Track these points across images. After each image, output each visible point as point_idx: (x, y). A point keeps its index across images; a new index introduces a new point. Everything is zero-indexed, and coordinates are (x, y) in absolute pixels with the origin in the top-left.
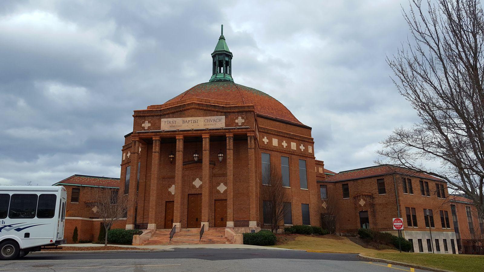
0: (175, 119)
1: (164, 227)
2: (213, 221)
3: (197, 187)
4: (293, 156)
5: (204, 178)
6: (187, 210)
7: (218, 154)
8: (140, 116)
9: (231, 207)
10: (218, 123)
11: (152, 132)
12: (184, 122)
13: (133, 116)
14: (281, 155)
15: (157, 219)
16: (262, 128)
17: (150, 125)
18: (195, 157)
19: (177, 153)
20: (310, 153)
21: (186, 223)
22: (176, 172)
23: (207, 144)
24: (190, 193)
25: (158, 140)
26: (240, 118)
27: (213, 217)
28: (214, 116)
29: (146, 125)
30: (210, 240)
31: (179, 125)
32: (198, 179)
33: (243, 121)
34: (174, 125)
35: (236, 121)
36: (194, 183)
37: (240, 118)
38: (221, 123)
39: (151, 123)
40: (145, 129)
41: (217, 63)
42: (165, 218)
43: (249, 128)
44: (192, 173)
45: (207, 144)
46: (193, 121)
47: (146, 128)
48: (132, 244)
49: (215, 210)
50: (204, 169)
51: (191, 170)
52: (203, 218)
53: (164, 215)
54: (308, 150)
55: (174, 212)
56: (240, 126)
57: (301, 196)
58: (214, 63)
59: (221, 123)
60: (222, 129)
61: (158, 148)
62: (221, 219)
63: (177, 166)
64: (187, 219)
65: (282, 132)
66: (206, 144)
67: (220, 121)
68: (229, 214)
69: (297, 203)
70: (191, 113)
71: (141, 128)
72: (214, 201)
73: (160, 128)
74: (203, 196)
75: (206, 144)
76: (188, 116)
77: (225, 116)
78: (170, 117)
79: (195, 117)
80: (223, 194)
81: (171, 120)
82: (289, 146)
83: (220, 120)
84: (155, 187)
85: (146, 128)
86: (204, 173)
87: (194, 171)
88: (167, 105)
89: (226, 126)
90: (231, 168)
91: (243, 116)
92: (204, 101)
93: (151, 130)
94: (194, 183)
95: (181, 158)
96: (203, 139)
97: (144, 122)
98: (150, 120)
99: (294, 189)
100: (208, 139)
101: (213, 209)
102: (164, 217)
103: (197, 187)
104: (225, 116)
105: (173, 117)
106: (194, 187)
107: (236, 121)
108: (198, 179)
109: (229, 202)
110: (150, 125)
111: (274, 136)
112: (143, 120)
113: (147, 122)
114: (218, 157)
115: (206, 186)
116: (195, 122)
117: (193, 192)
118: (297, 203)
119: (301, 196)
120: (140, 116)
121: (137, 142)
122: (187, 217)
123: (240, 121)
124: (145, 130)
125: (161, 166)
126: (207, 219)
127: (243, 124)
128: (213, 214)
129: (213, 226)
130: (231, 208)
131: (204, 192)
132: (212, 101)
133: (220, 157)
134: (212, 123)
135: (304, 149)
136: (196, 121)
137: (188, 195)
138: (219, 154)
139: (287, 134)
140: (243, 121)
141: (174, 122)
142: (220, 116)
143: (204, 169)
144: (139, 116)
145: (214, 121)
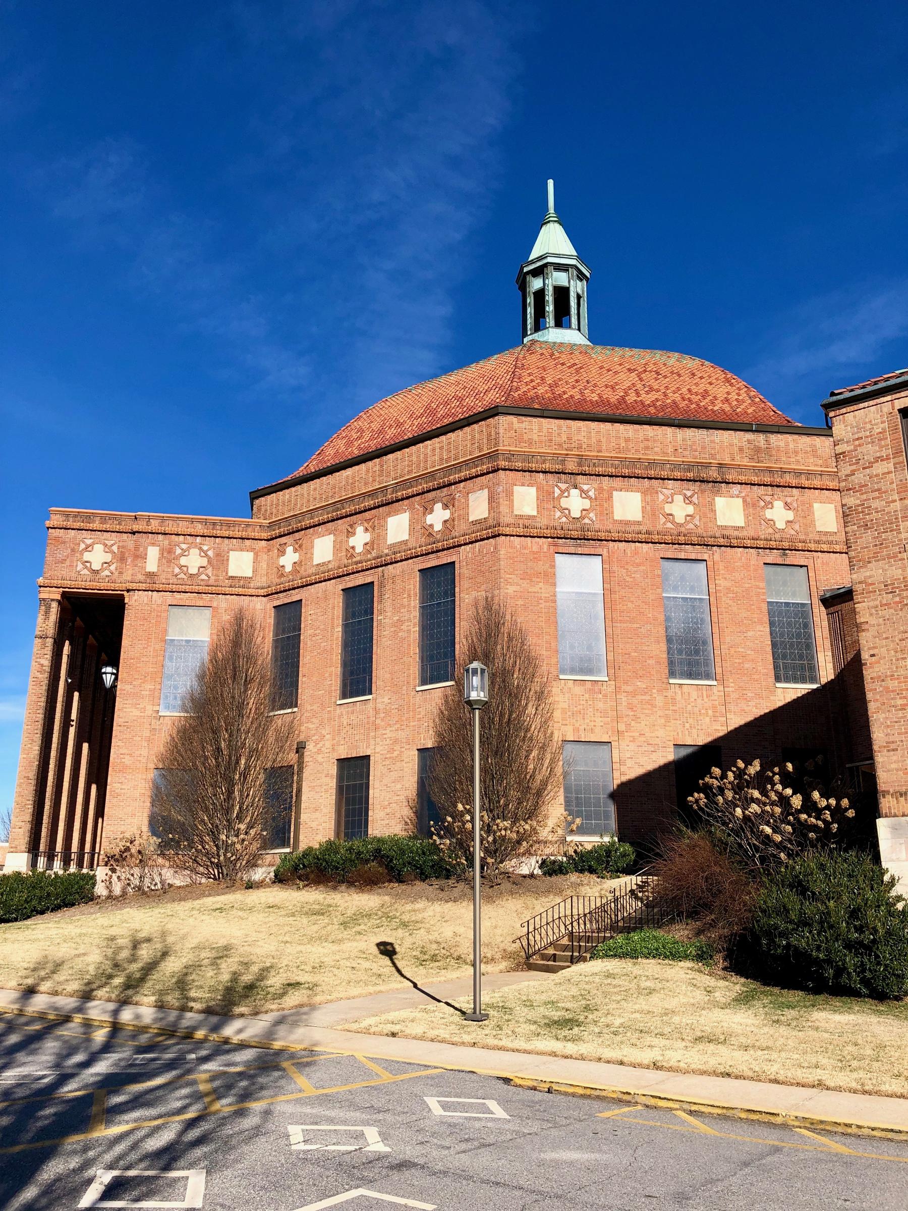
14: (341, 587)
69: (396, 753)
99: (386, 700)
111: (320, 529)
118: (396, 753)
133: (109, 676)
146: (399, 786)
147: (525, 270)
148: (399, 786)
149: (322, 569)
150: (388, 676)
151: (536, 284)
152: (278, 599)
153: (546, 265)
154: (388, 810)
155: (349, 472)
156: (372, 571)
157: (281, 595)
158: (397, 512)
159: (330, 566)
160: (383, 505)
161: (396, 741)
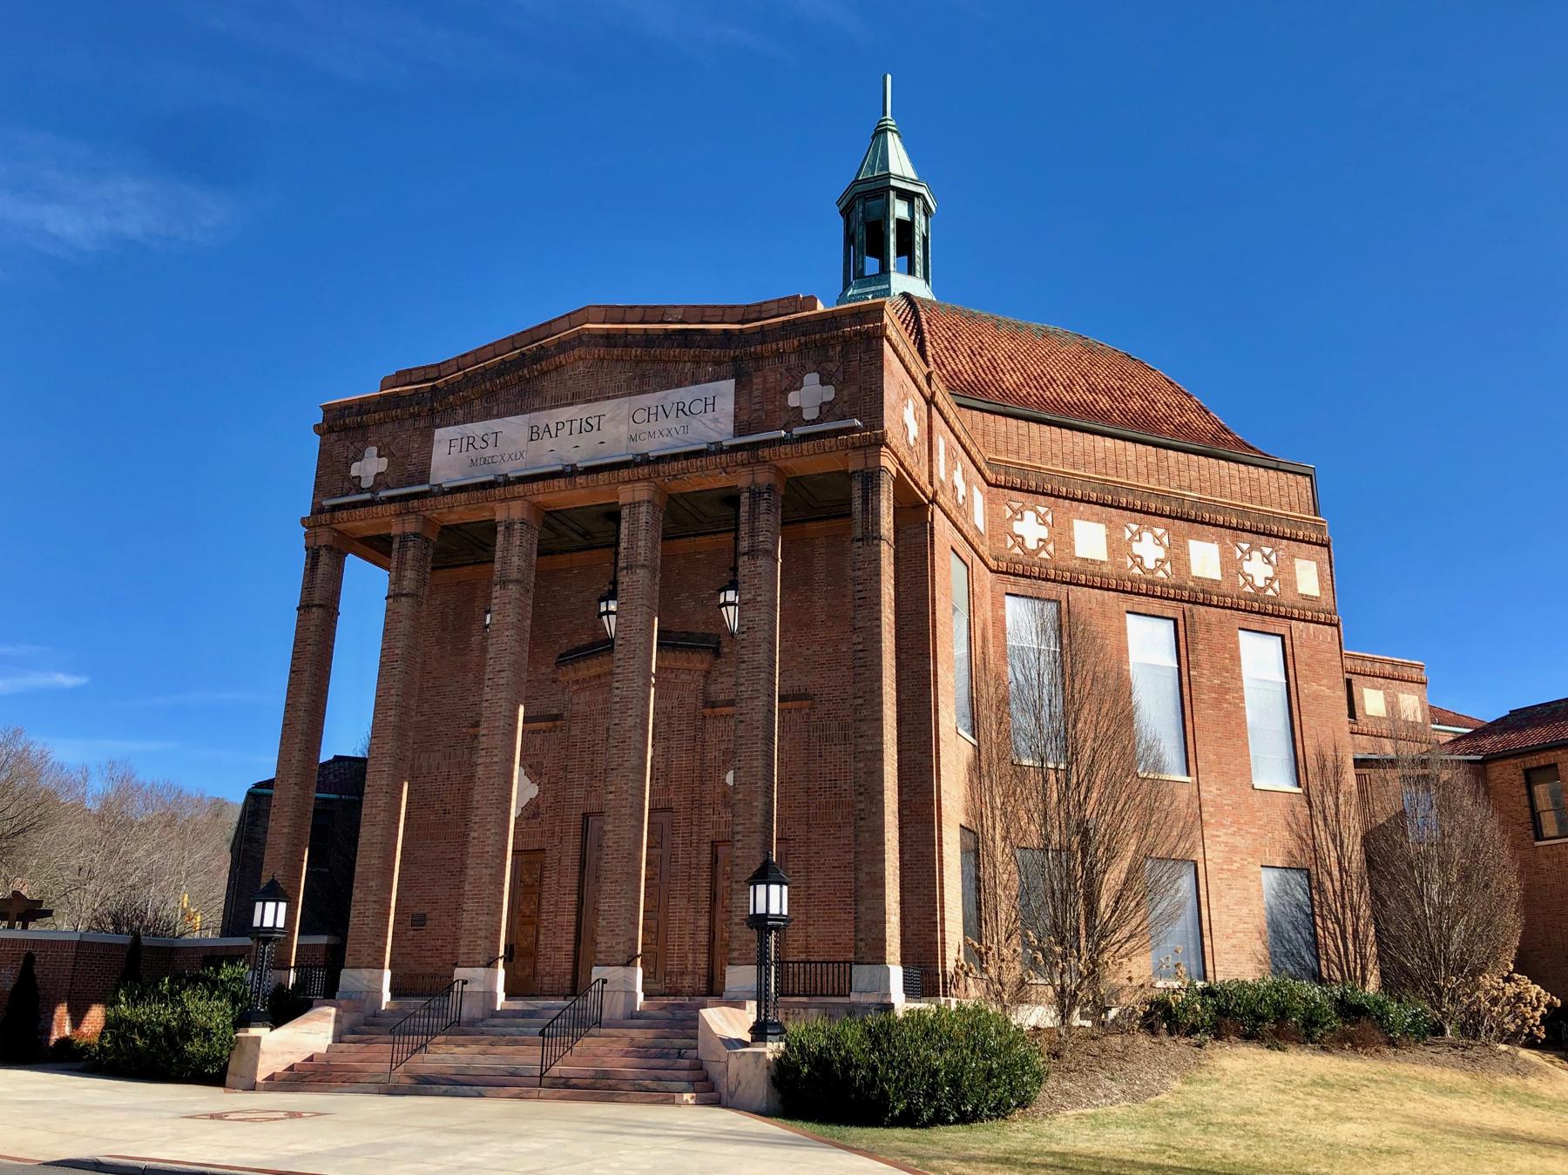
0: (495, 424)
2: (702, 960)
4: (1202, 609)
7: (720, 591)
8: (346, 428)
10: (704, 413)
11: (391, 500)
12: (534, 434)
13: (317, 428)
14: (1125, 607)
15: (439, 943)
16: (1007, 467)
17: (381, 465)
19: (497, 591)
20: (1305, 597)
21: (568, 966)
22: (488, 693)
23: (642, 535)
25: (416, 535)
26: (811, 379)
27: (703, 938)
28: (679, 385)
29: (370, 466)
30: (606, 1075)
31: (513, 450)
33: (829, 393)
34: (489, 452)
35: (793, 399)
37: (811, 379)
38: (716, 420)
39: (390, 455)
40: (364, 485)
41: (861, 235)
43: (854, 429)
45: (642, 535)
46: (576, 425)
47: (367, 483)
48: (229, 1078)
49: (713, 898)
52: (603, 941)
54: (1291, 583)
56: (813, 422)
57: (1261, 827)
58: (849, 238)
59: (716, 420)
60: (715, 450)
61: (409, 574)
64: (570, 947)
65: (1131, 490)
66: (632, 536)
67: (710, 408)
69: (1235, 866)
70: (570, 383)
71: (347, 485)
72: (706, 848)
73: (423, 476)
75: (632, 536)
76: (559, 402)
77: (730, 384)
78: (469, 418)
79: (590, 401)
81: (476, 429)
82: (1177, 556)
83: (710, 404)
85: (367, 483)
88: (469, 360)
89: (739, 430)
91: (831, 366)
92: (638, 314)
93: (388, 488)
95: (512, 619)
96: (625, 512)
97: (359, 456)
98: (386, 440)
99: (1213, 789)
100: (643, 509)
101: (704, 894)
104: (730, 384)
105: (488, 415)
107: (793, 399)
109: (739, 853)
110: (381, 465)
111: (1082, 506)
112: (358, 445)
113: (375, 450)
114: (721, 606)
116: (588, 426)
118: (1235, 866)
119: (1261, 827)
120: (346, 428)
121: (323, 552)
122: (572, 936)
123: (810, 395)
124: (361, 491)
126: (621, 947)
127: (825, 409)
128: (704, 922)
129: (702, 986)
131: (611, 796)
132: (673, 311)
133: (731, 609)
134: (671, 423)
135: (1271, 574)
136: (594, 422)
137: (585, 816)
138: (724, 589)
139: (1164, 497)
140: (829, 393)
141: (491, 441)
142: (710, 381)
144: (344, 427)
145: (681, 409)
146: (1245, 910)
147: (893, 183)
148: (1245, 910)
149: (1091, 567)
150: (1212, 757)
151: (900, 210)
152: (1015, 584)
153: (918, 195)
154: (1234, 941)
155: (1109, 442)
156: (1174, 603)
157: (1023, 581)
158: (1200, 538)
159: (1105, 570)
160: (1181, 519)
161: (1233, 849)
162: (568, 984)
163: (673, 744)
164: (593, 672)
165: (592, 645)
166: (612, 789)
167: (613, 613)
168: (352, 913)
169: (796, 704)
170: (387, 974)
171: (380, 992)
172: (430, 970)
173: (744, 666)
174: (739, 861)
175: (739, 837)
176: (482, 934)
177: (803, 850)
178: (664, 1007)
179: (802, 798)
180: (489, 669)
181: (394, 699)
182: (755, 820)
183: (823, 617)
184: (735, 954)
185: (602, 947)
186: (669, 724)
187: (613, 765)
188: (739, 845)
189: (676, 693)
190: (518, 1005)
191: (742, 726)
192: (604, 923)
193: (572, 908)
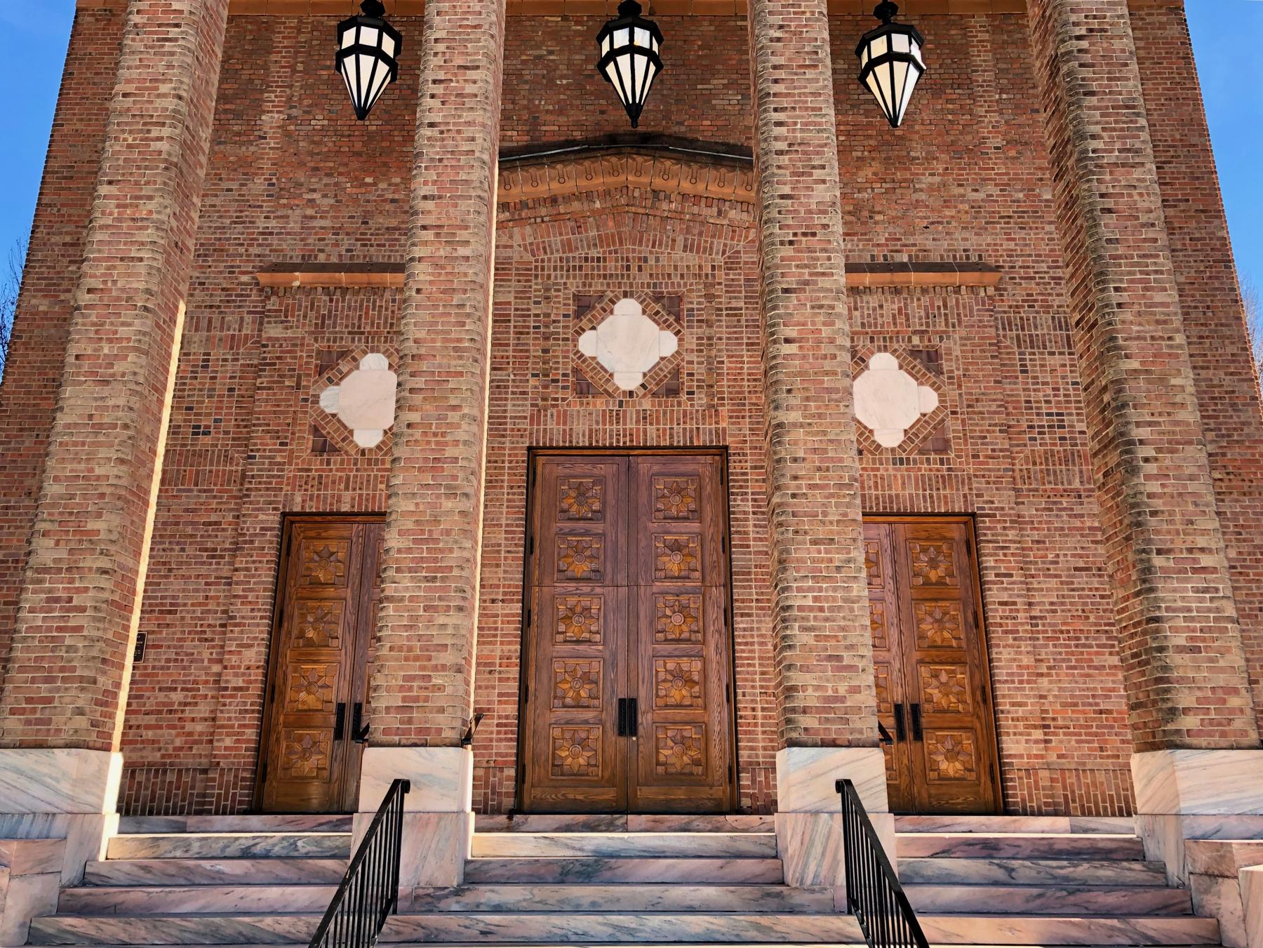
1: (242, 794)
3: (628, 379)
5: (786, 190)
6: (517, 608)
9: (1201, 542)
15: (177, 697)
18: (631, 49)
24: (552, 431)
32: (627, 309)
36: (588, 344)
42: (271, 692)
44: (568, 246)
50: (780, 88)
51: (557, 218)
53: (254, 655)
55: (390, 589)
62: (924, 721)
63: (441, 47)
64: (512, 709)
68: (1181, 640)
74: (794, 400)
80: (899, 458)
84: (141, 268)
86: (782, 131)
87: (593, 233)
90: (1119, 86)
94: (588, 344)
102: (257, 675)
103: (628, 379)
106: (588, 381)
108: (627, 309)
109: (1154, 487)
115: (823, 282)
117: (582, 423)
122: (513, 687)
125: (259, 180)
130: (1206, 561)
131: (791, 349)
137: (532, 452)
143: (780, 88)
162: (509, 786)
163: (722, 329)
164: (543, 190)
165: (527, 149)
166: (791, 332)
167: (642, 51)
168: (31, 598)
169: (971, 277)
170: (116, 762)
171: (98, 813)
172: (156, 757)
173: (1093, 100)
174: (1158, 504)
175: (1149, 451)
176: (448, 658)
177: (1011, 534)
178: (946, 851)
179: (1000, 441)
180: (434, 61)
181: (171, 104)
182: (1182, 415)
183: (999, 141)
184: (1189, 722)
185: (808, 698)
186: (710, 297)
187: (791, 282)
188: (1152, 468)
189: (718, 244)
190: (526, 844)
191: (1107, 219)
192: (808, 638)
193: (513, 628)
